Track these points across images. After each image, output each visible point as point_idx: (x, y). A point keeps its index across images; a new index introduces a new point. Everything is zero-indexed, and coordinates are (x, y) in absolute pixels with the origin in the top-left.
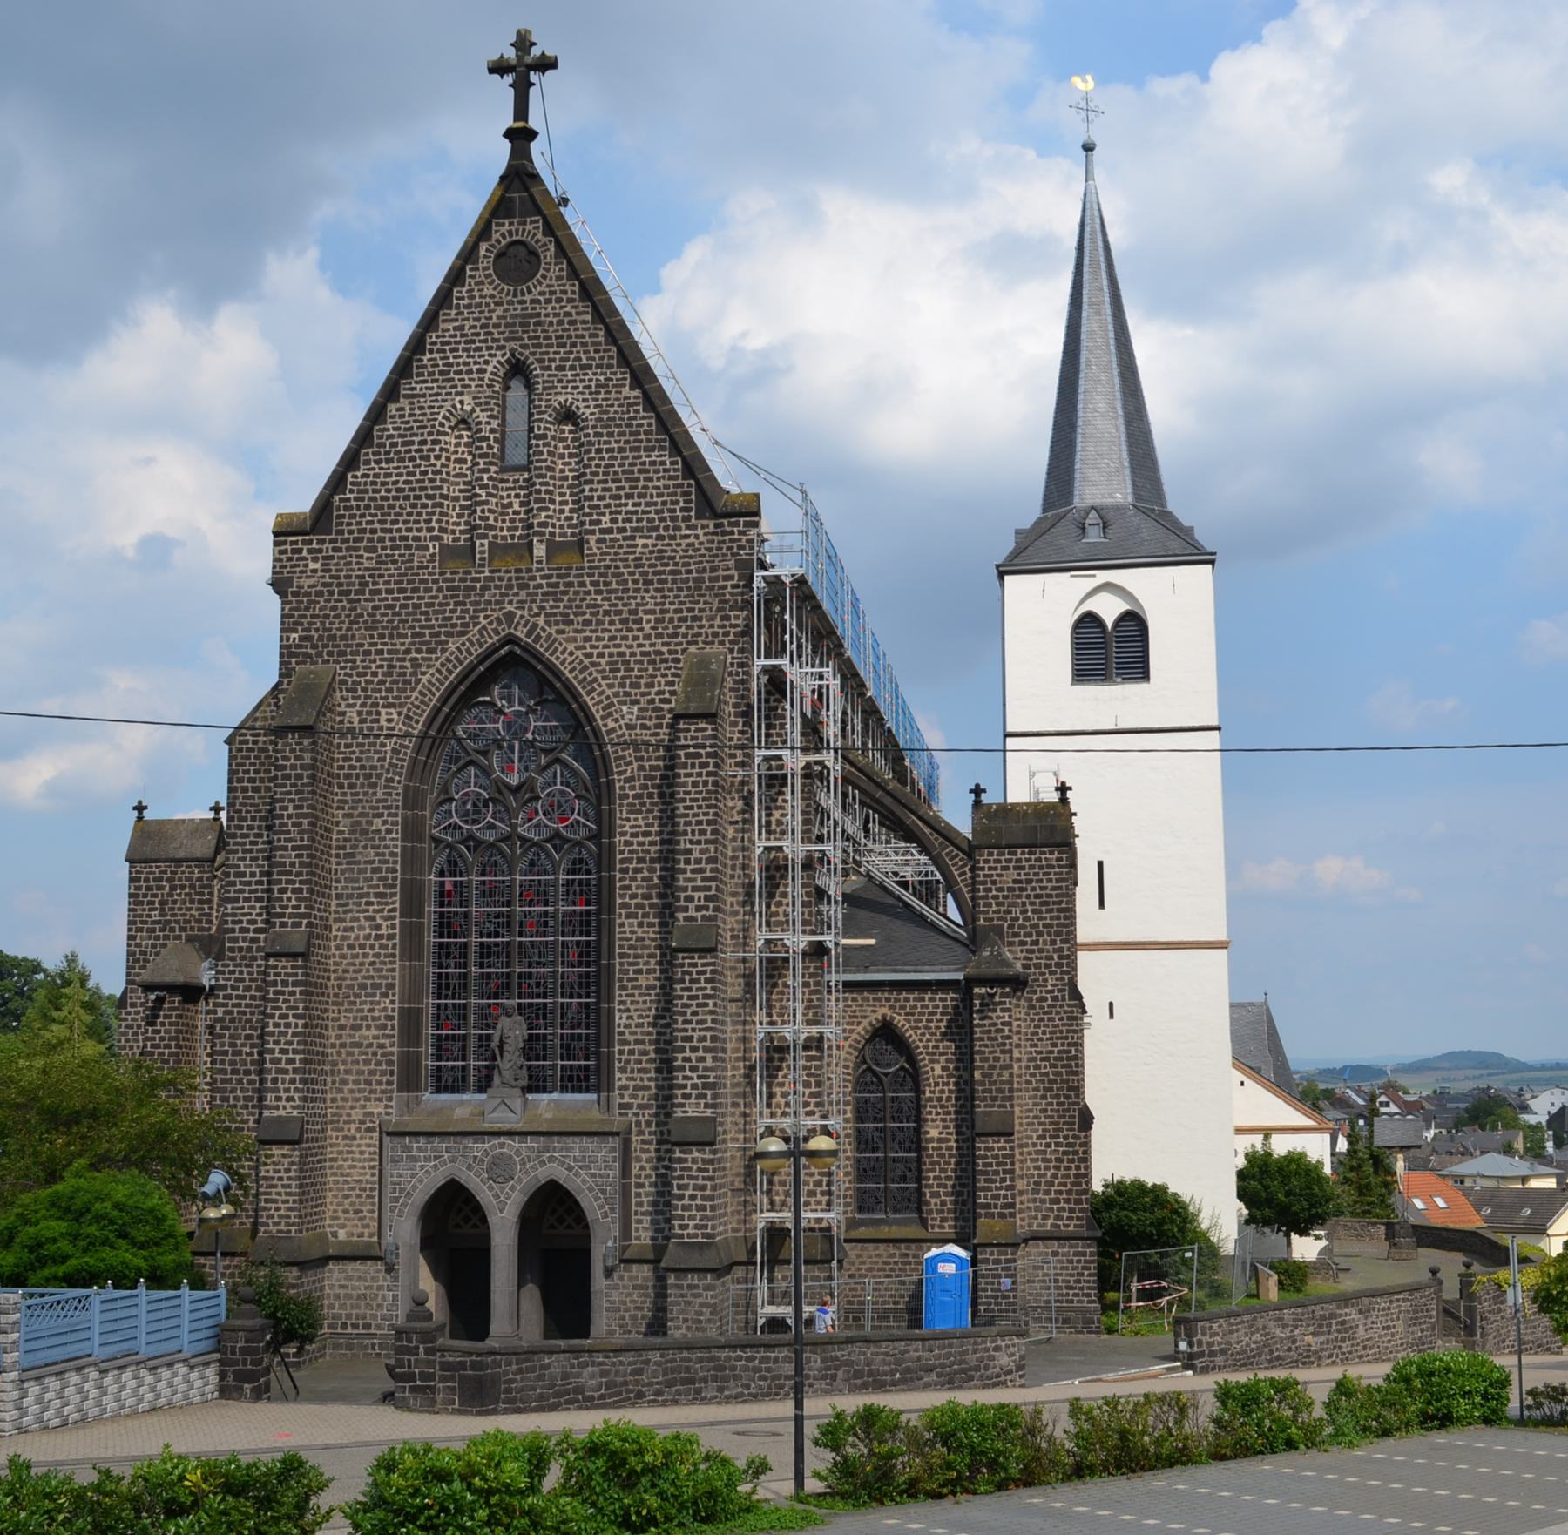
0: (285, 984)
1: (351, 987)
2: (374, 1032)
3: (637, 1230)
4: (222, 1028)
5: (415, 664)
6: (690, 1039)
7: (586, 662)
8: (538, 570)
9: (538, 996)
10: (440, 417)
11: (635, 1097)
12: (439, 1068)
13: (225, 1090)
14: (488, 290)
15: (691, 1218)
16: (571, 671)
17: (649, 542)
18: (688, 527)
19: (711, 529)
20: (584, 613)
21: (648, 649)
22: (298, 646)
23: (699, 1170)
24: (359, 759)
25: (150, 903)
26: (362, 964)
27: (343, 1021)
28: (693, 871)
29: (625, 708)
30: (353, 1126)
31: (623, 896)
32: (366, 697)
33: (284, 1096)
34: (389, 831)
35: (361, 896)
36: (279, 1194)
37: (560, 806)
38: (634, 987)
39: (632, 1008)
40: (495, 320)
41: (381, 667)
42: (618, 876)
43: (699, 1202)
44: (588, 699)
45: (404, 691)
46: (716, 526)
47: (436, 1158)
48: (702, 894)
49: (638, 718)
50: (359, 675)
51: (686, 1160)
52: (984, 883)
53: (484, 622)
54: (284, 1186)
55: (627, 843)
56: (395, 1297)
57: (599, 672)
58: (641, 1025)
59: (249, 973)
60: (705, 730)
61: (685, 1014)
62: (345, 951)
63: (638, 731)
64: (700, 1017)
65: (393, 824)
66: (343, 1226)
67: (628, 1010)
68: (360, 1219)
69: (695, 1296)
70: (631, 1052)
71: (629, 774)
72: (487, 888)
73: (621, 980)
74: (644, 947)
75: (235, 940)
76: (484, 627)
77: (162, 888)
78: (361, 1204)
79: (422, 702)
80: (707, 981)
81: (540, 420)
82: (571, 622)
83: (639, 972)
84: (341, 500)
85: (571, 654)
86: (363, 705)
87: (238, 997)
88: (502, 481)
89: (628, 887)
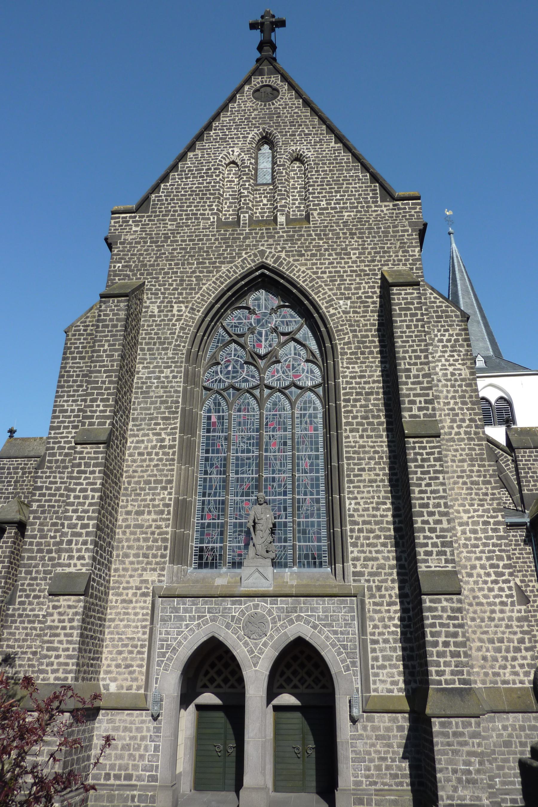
0: (87, 465)
1: (138, 483)
2: (153, 516)
3: (375, 682)
4: (34, 518)
5: (198, 278)
6: (427, 506)
7: (314, 276)
8: (280, 229)
9: (280, 494)
10: (220, 158)
11: (366, 566)
12: (201, 549)
13: (30, 566)
14: (249, 104)
15: (446, 664)
16: (304, 282)
17: (352, 214)
18: (376, 206)
19: (391, 207)
20: (312, 250)
21: (355, 268)
22: (120, 271)
23: (449, 618)
24: (156, 334)
25: (8, 482)
26: (148, 466)
27: (129, 508)
28: (413, 383)
29: (341, 302)
30: (130, 592)
31: (346, 417)
32: (164, 298)
33: (76, 555)
34: (175, 377)
35: (151, 419)
36: (60, 642)
37: (294, 368)
38: (359, 481)
39: (359, 496)
40: (253, 116)
41: (176, 280)
42: (343, 404)
43: (452, 648)
44: (316, 297)
45: (191, 294)
46: (394, 205)
47: (199, 617)
48: (422, 399)
49: (351, 307)
50: (159, 285)
51: (436, 609)
52: (524, 469)
53: (245, 256)
54: (66, 635)
55: (347, 383)
56: (156, 748)
57: (322, 282)
58: (367, 509)
59: (61, 478)
60: (413, 293)
61: (420, 485)
62: (136, 457)
63: (351, 315)
64: (433, 488)
65: (177, 372)
66: (114, 680)
67: (356, 498)
68: (131, 673)
69: (461, 744)
70: (360, 531)
71: (346, 340)
72: (242, 420)
73: (348, 476)
74: (365, 452)
75: (54, 455)
76: (245, 259)
77: (18, 473)
78: (132, 659)
79: (202, 300)
80: (435, 460)
81: (281, 158)
82: (303, 255)
83: (363, 470)
84: (156, 197)
85: (304, 272)
86: (162, 302)
87: (50, 495)
88: (256, 190)
89: (351, 412)
